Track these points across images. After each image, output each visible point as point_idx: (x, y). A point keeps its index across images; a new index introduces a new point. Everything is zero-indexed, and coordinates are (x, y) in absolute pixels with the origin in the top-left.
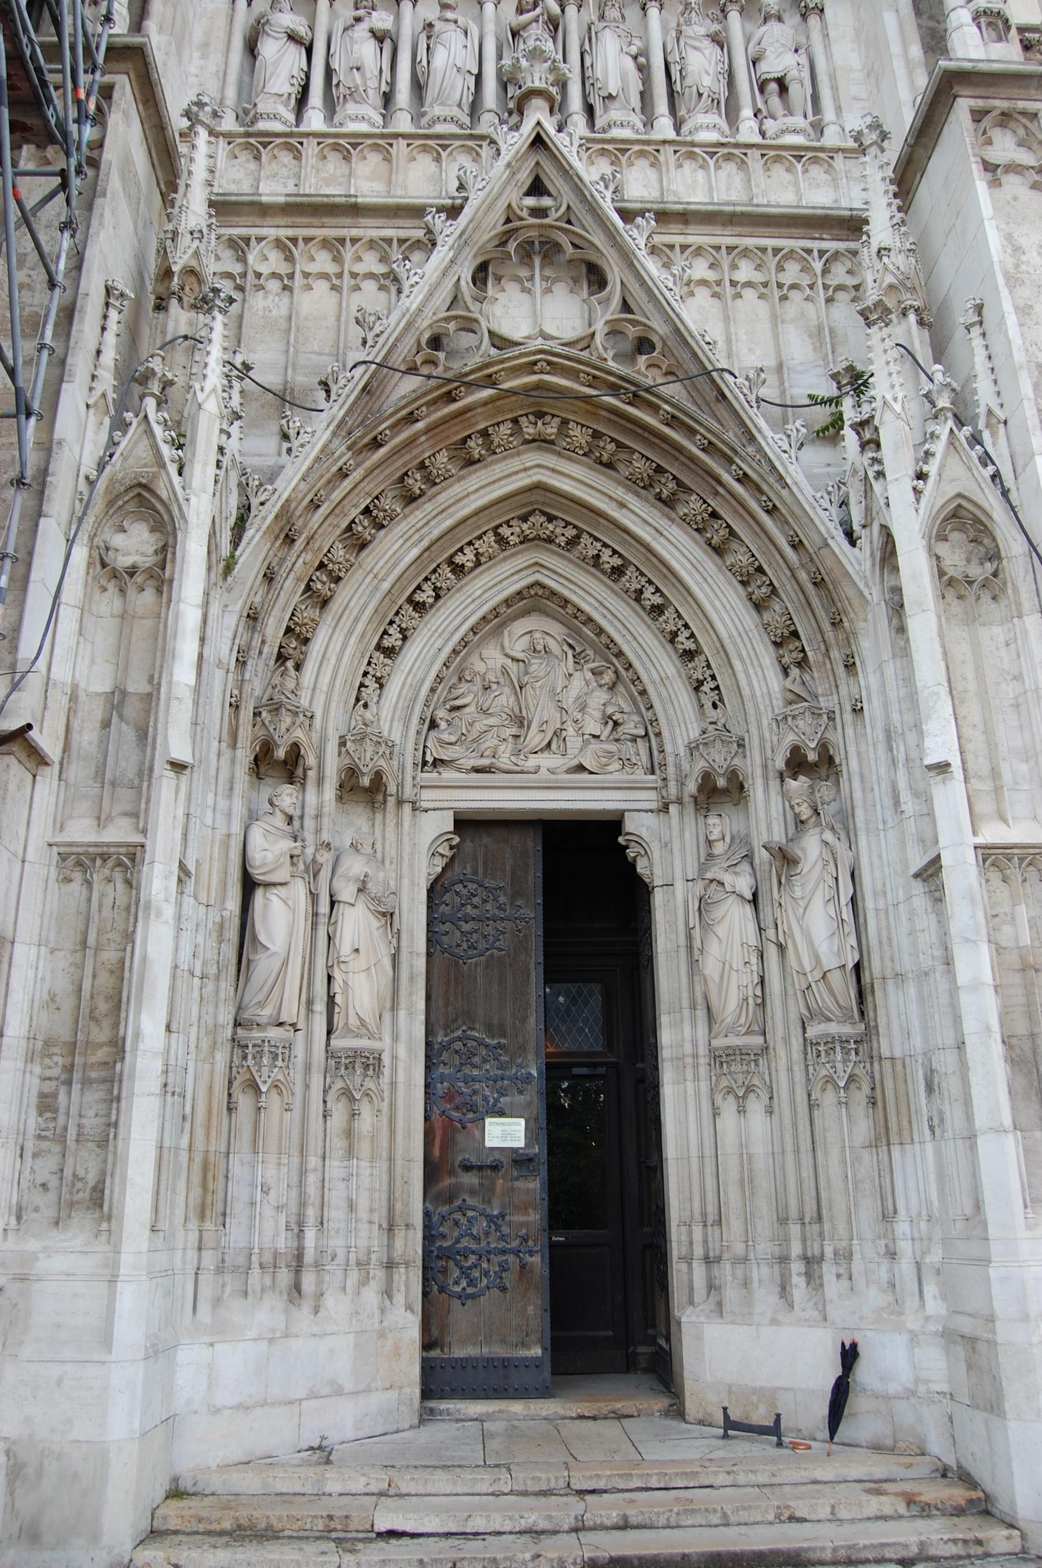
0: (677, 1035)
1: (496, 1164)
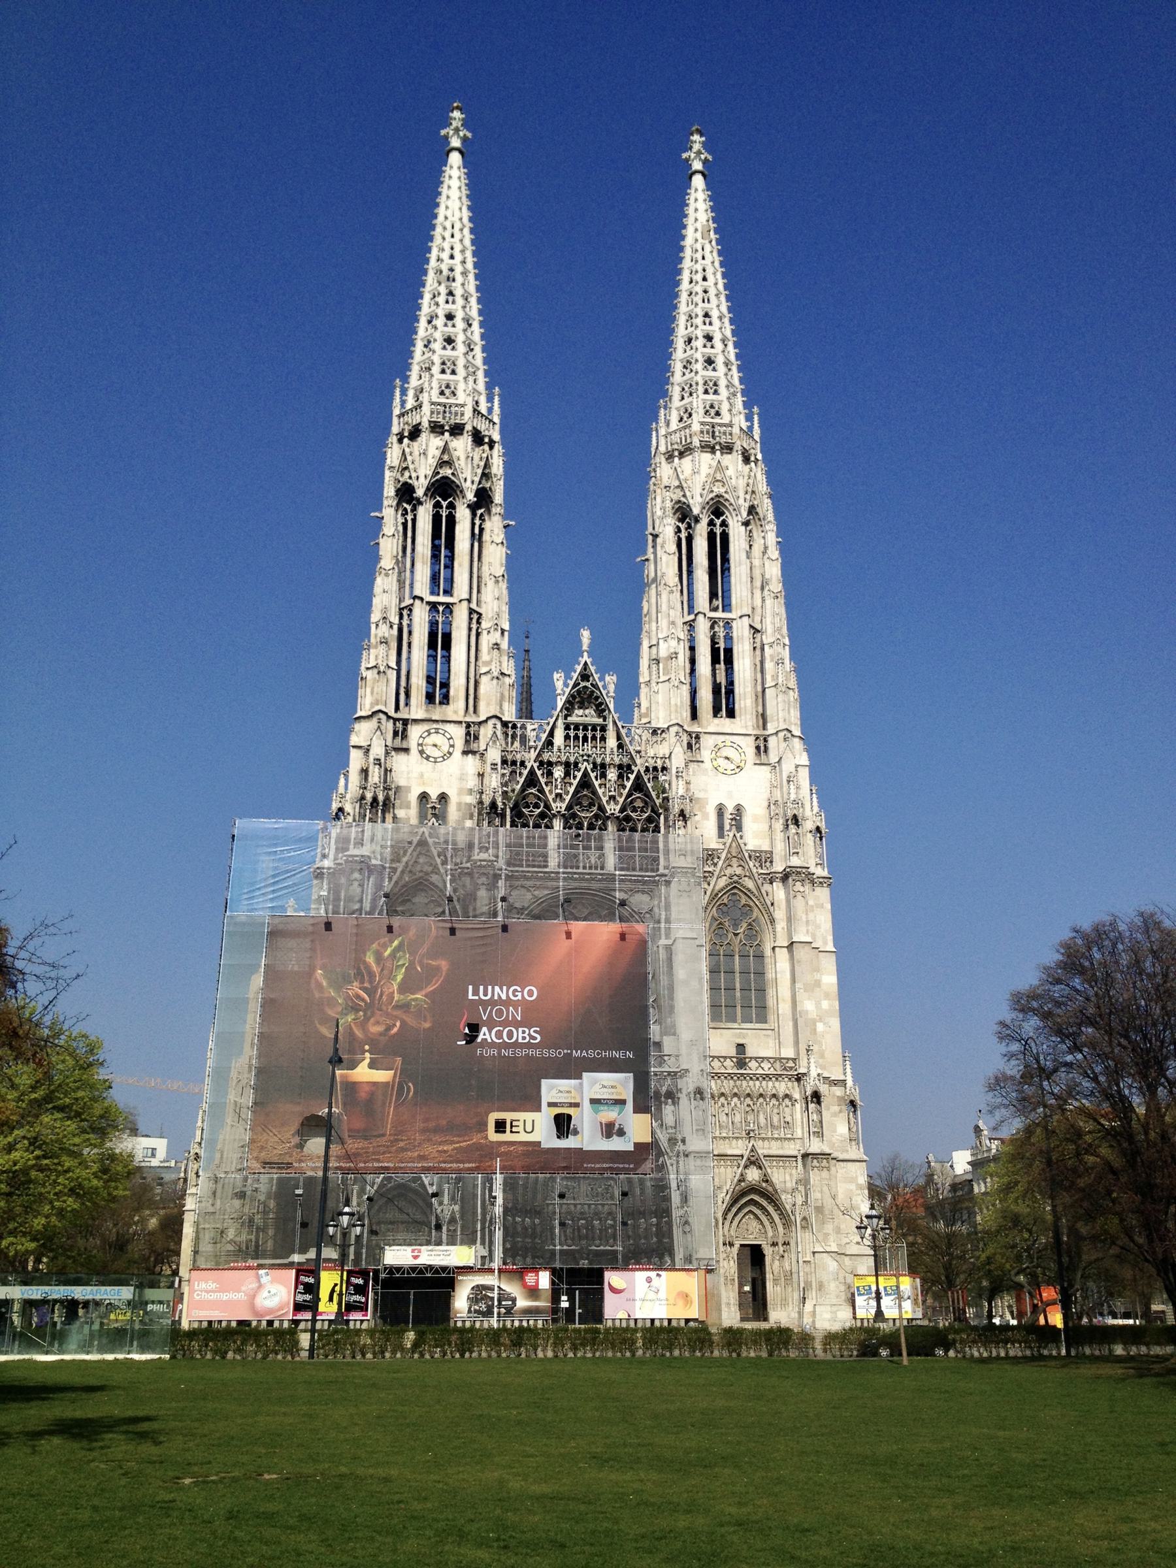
0: (769, 1276)
1: (745, 1293)
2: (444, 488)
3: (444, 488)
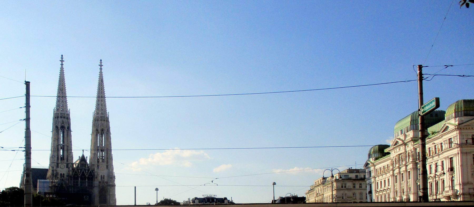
2: (63, 127)
3: (63, 127)
